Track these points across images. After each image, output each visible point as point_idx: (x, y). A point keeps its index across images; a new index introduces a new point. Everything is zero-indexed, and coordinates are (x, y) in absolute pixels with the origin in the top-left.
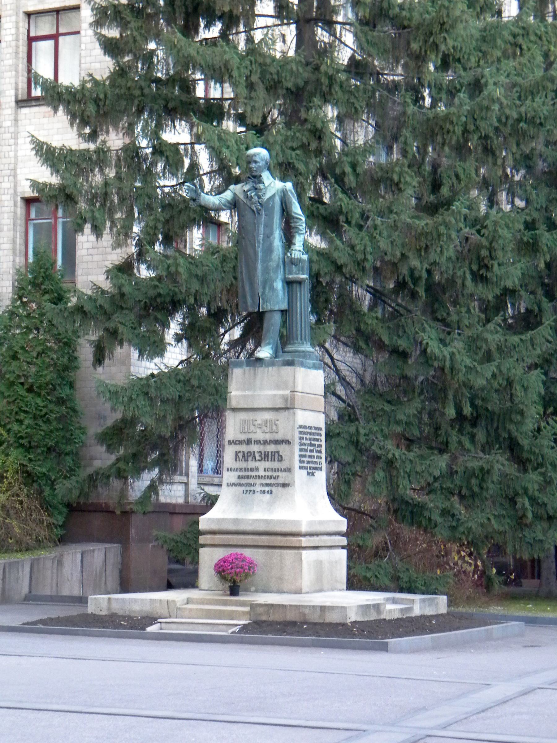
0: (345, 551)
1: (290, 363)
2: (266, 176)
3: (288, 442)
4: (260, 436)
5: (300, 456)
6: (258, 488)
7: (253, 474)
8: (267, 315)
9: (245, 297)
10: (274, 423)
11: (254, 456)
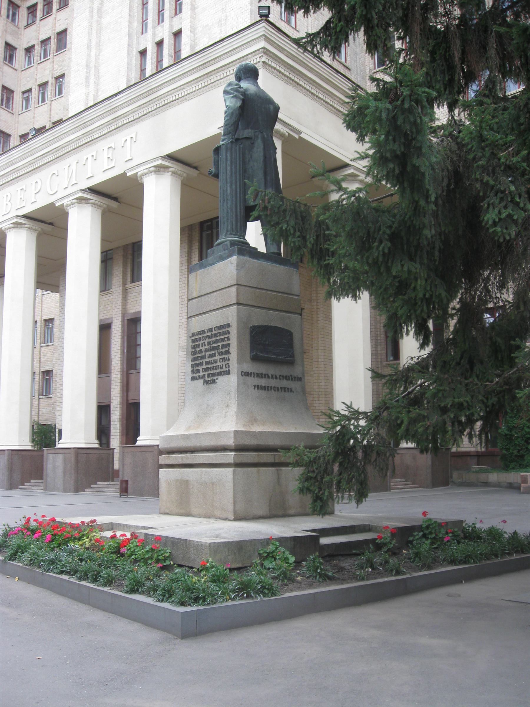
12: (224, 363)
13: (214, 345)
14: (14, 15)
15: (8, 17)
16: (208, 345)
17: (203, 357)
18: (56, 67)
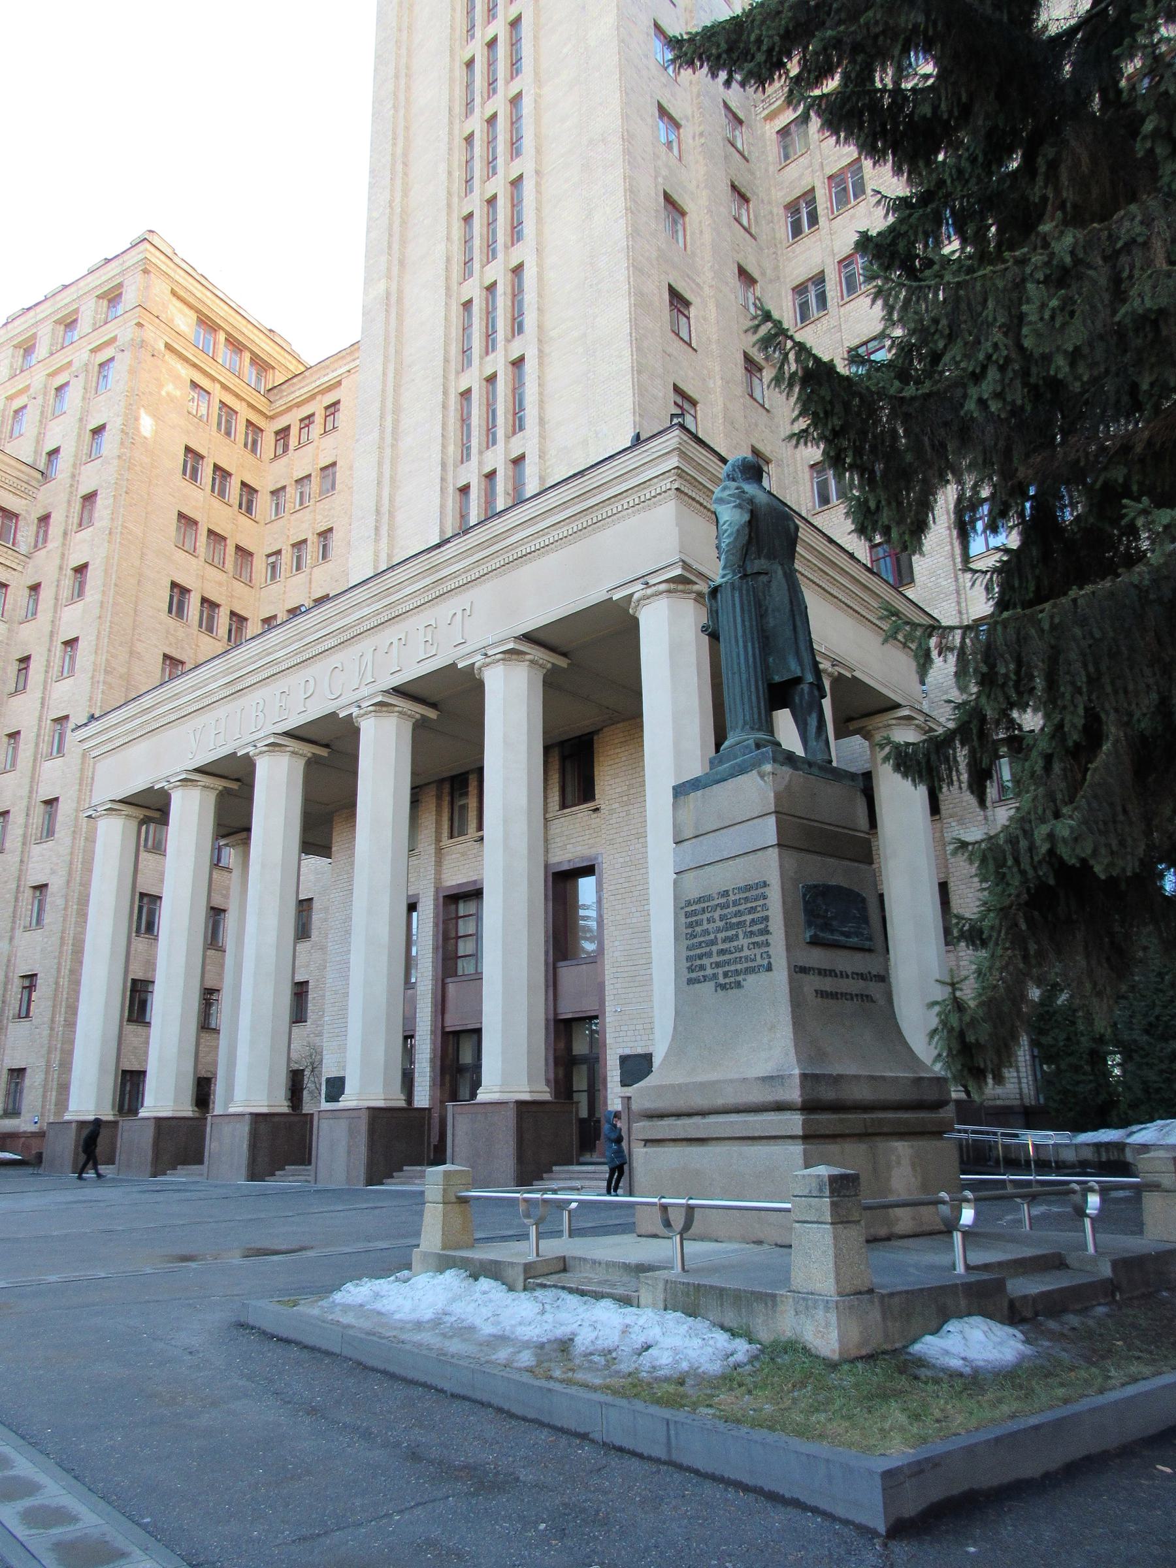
12: (758, 951)
13: (734, 920)
14: (255, 442)
15: (246, 445)
16: (721, 920)
17: (713, 942)
18: (319, 517)
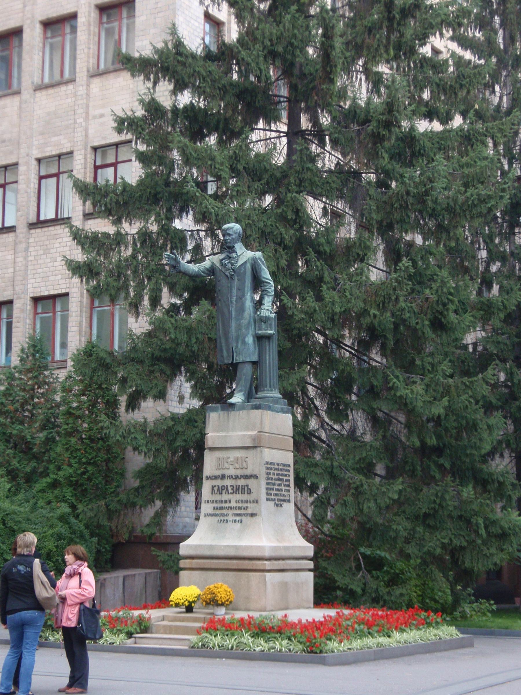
0: (312, 574)
1: (257, 407)
2: (239, 247)
3: (256, 477)
4: (232, 472)
5: (267, 489)
6: (230, 518)
7: (226, 505)
8: (240, 367)
9: (222, 350)
10: (244, 460)
11: (227, 490)
17: (274, 484)
